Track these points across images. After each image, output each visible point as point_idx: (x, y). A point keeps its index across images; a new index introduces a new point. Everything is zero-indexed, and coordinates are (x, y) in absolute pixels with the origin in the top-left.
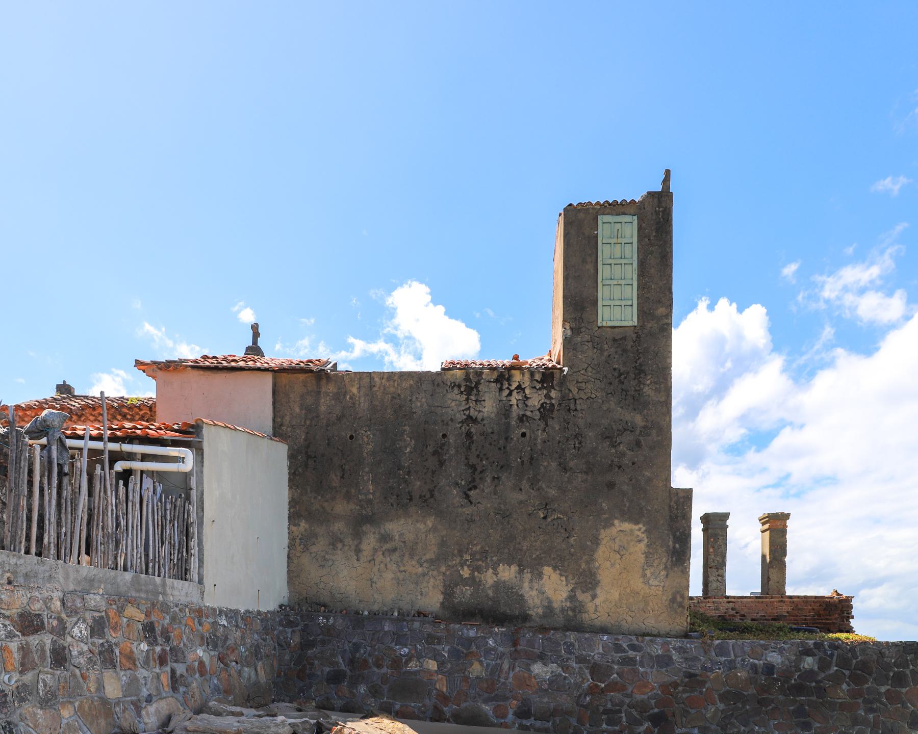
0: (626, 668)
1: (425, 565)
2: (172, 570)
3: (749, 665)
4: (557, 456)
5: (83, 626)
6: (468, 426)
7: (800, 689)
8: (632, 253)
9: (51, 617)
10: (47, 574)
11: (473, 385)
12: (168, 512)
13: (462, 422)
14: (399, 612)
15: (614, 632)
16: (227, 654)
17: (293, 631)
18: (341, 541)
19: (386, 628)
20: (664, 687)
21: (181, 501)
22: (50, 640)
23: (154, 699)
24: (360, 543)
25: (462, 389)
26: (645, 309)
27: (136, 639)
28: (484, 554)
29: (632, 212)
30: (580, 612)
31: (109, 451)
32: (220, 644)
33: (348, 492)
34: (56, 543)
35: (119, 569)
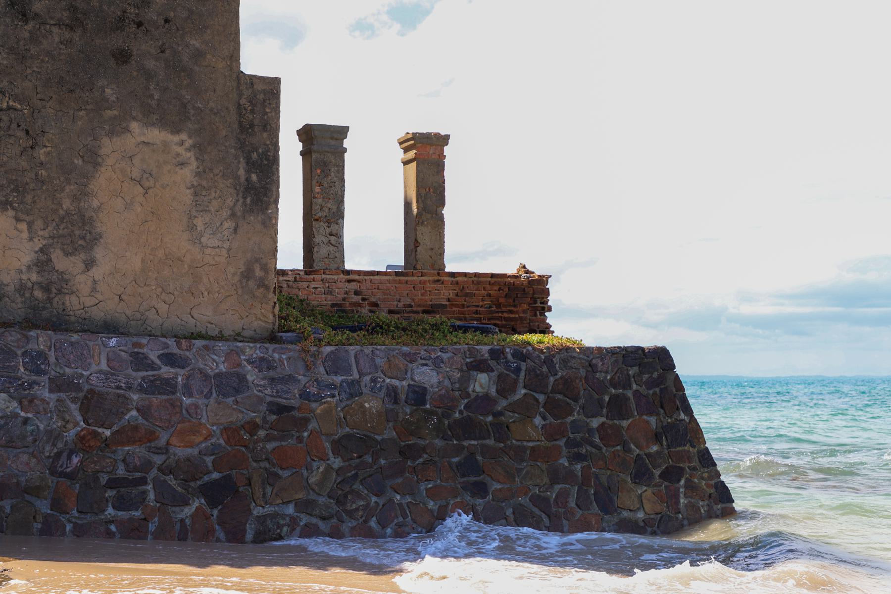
0: (156, 399)
3: (384, 390)
7: (467, 428)
15: (131, 331)
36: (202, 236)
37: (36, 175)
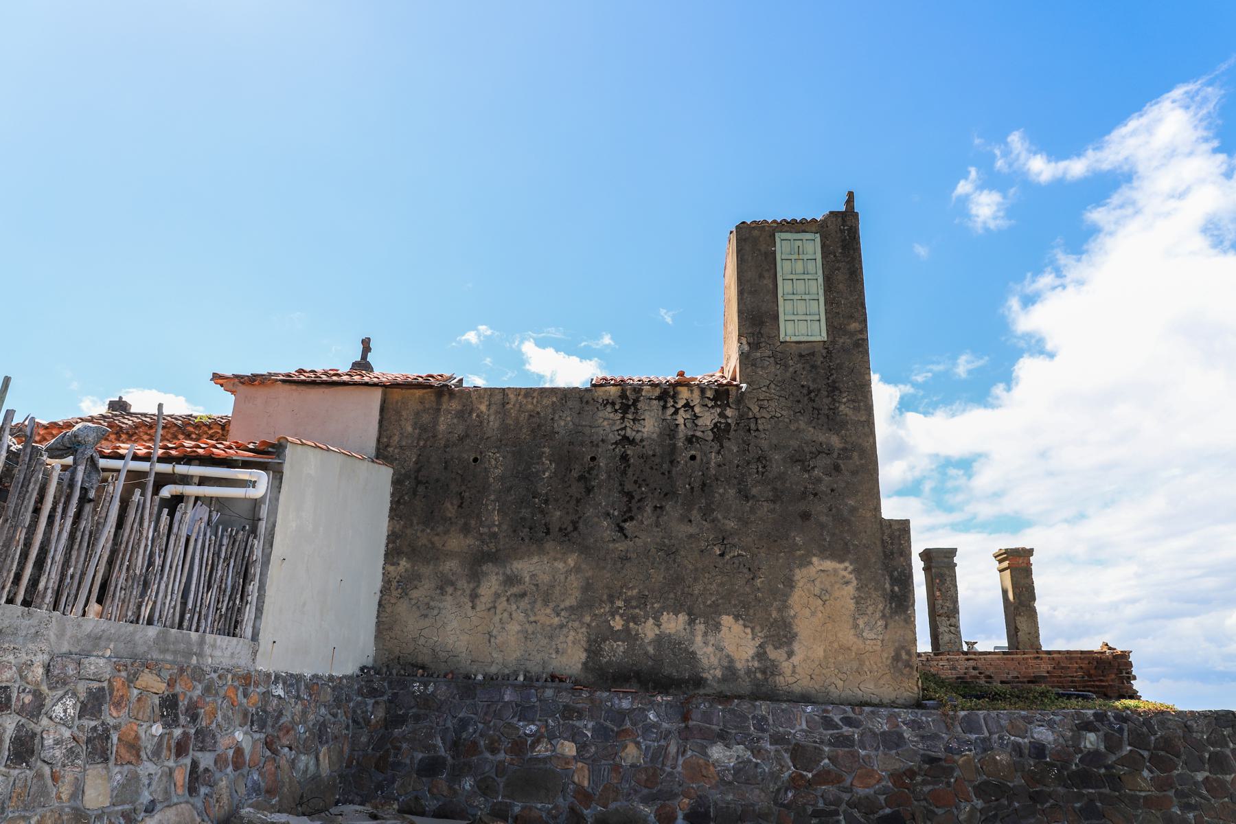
0: (841, 751)
1: (563, 613)
2: (216, 623)
3: (1010, 746)
4: (735, 481)
5: (70, 703)
6: (624, 447)
7: (1083, 778)
8: (816, 269)
9: (24, 690)
10: (33, 631)
11: (630, 403)
12: (224, 549)
13: (616, 443)
14: (525, 675)
15: (820, 700)
16: (278, 737)
17: (376, 703)
18: (452, 584)
19: (507, 698)
20: (896, 777)
21: (243, 534)
22: (15, 724)
23: (159, 806)
24: (478, 586)
25: (617, 407)
26: (835, 324)
27: (146, 719)
28: (643, 600)
29: (814, 229)
30: (772, 674)
31: (156, 473)
32: (270, 722)
33: (466, 524)
34: (56, 588)
35: (141, 622)
36: (863, 632)
37: (756, 596)
